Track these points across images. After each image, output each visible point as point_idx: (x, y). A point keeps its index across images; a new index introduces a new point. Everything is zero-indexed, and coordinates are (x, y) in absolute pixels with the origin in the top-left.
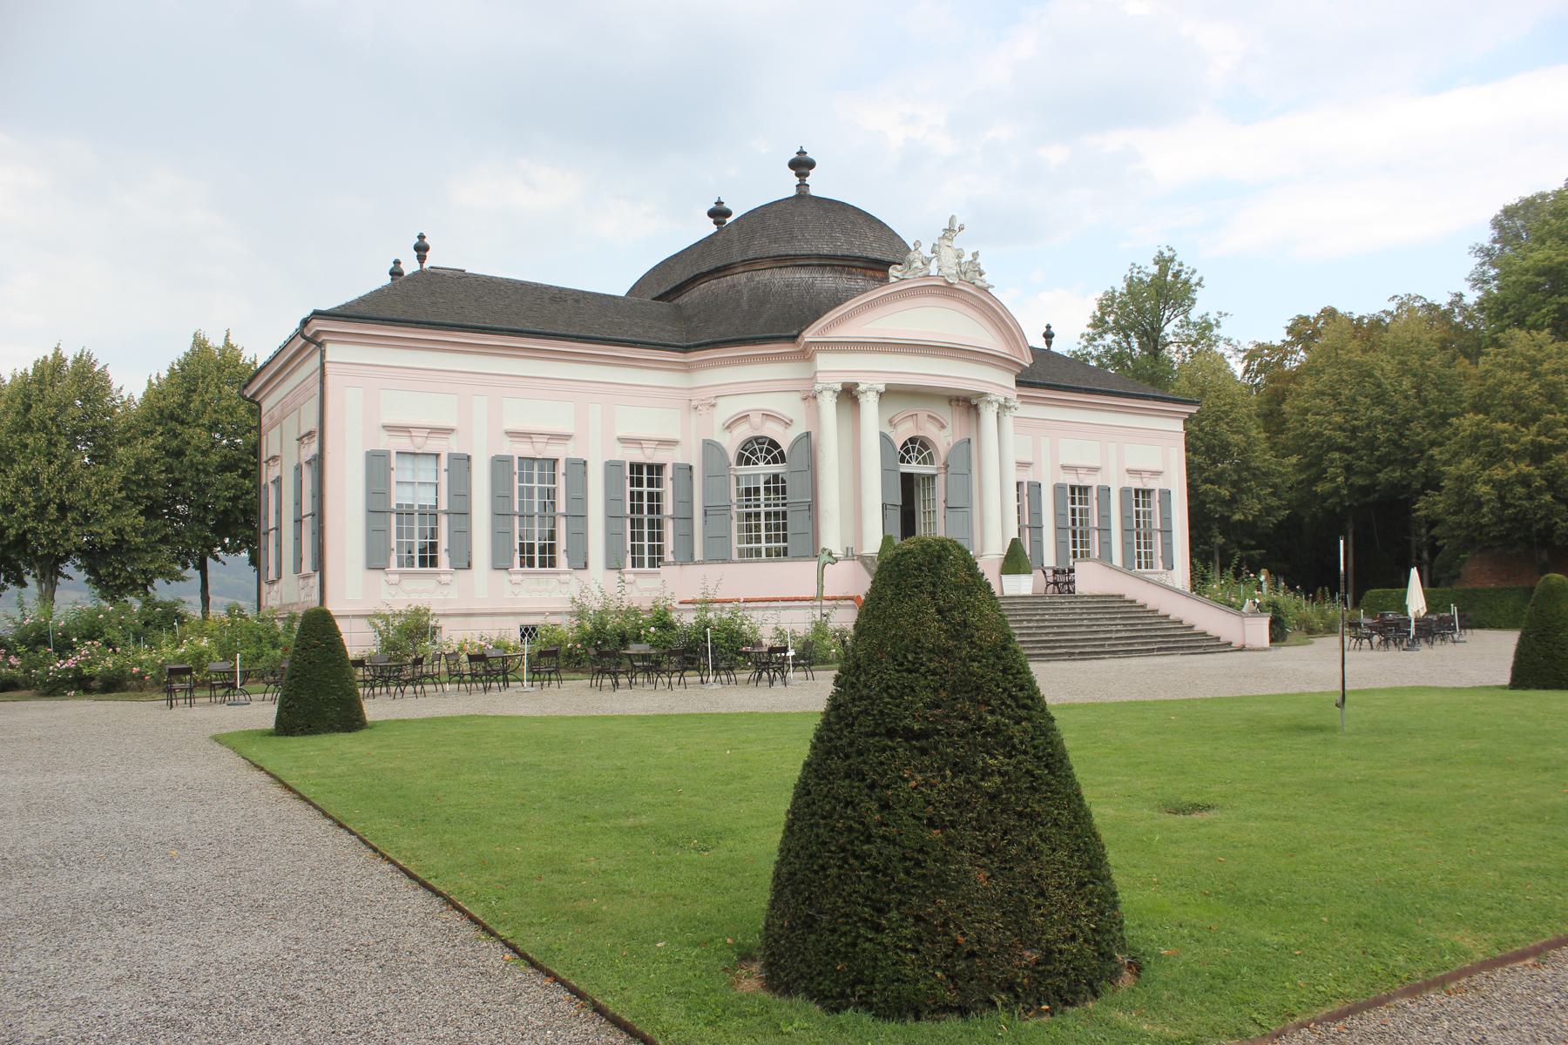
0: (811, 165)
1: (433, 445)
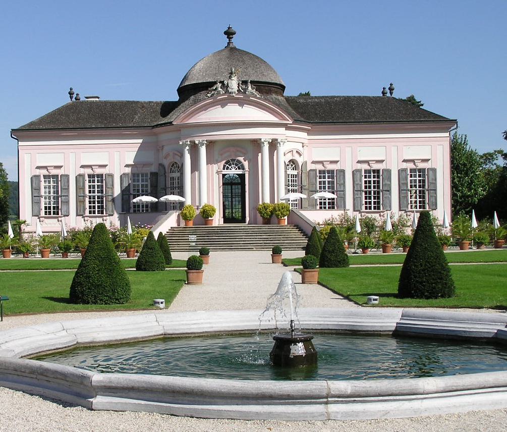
0: (234, 33)
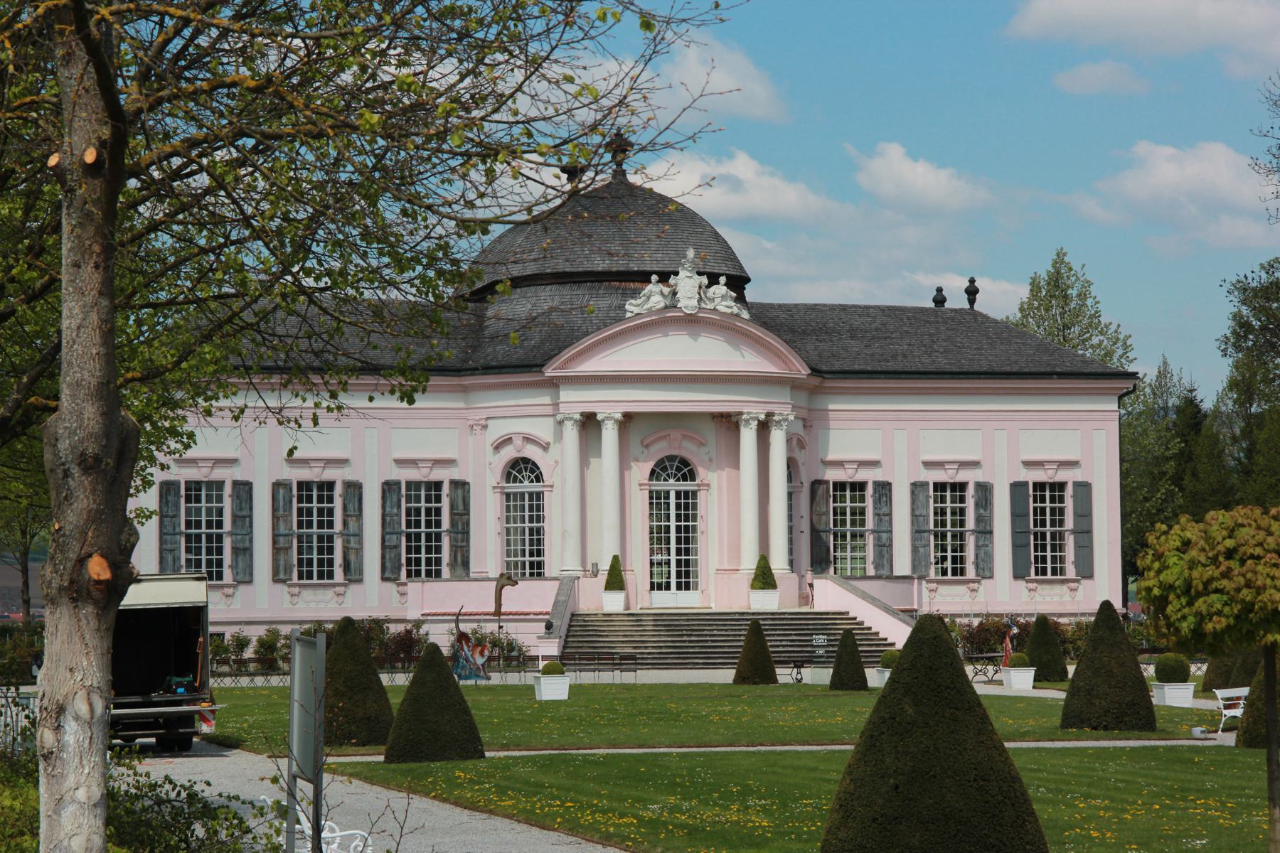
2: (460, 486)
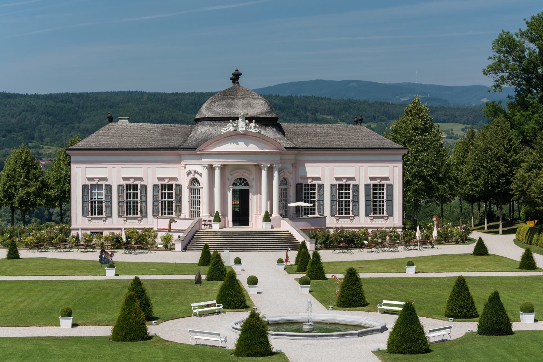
0: (241, 74)
1: (100, 183)
2: (177, 185)
